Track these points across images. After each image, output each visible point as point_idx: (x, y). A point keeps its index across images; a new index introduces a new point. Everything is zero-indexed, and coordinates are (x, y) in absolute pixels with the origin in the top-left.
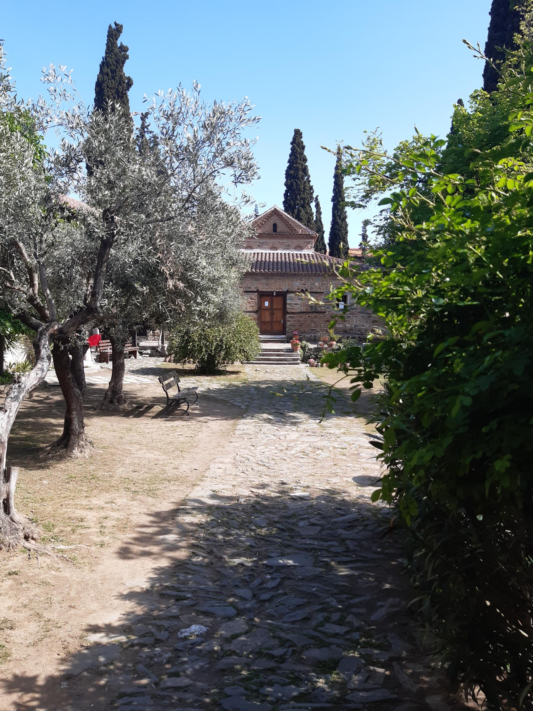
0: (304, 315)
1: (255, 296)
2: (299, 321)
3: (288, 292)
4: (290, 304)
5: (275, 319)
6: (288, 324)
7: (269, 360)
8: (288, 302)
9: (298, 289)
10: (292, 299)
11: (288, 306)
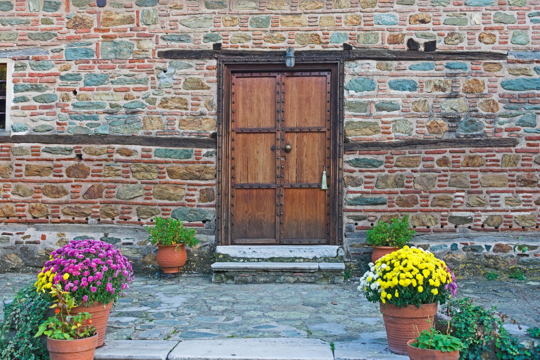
0: (422, 152)
1: (206, 72)
3: (349, 53)
5: (292, 176)
6: (350, 193)
9: (394, 40)
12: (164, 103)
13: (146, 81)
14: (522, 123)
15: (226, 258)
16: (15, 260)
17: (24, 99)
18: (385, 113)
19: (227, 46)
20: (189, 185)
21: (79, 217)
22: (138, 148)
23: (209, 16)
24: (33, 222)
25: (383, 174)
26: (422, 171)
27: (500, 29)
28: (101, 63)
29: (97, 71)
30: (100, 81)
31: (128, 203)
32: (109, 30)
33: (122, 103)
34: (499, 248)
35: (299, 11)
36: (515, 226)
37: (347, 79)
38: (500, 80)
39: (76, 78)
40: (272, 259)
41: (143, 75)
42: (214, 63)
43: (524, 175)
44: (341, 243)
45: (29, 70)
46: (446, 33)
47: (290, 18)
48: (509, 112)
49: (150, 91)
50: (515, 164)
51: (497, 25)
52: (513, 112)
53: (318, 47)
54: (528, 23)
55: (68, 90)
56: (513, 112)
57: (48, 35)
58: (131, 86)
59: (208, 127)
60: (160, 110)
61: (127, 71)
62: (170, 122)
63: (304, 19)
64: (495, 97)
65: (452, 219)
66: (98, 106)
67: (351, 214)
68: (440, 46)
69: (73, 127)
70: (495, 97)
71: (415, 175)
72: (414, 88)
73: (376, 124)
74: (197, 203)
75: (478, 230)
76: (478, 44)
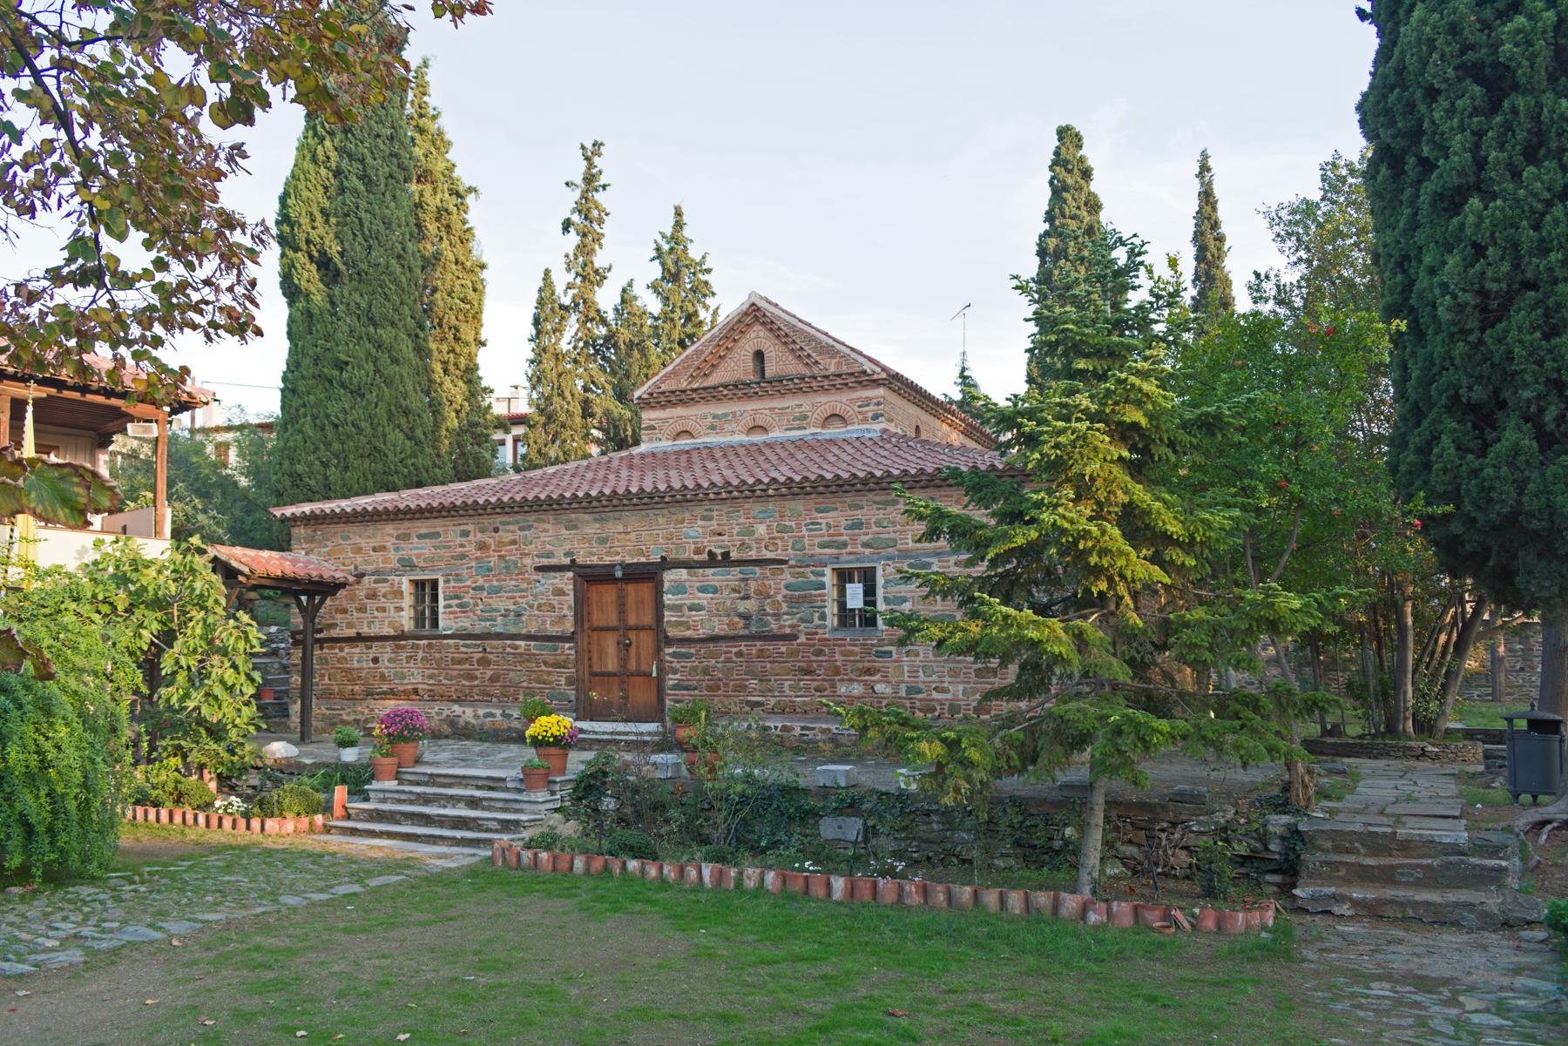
0: (723, 646)
1: (566, 581)
2: (706, 671)
3: (666, 564)
4: (676, 608)
5: (632, 665)
6: (671, 680)
7: (426, 820)
8: (668, 599)
9: (698, 551)
10: (680, 589)
11: (668, 616)
12: (539, 607)
13: (525, 590)
14: (802, 620)
16: (446, 729)
17: (449, 606)
19: (580, 561)
21: (486, 698)
22: (522, 643)
24: (457, 701)
27: (781, 538)
30: (498, 590)
31: (517, 686)
33: (512, 607)
34: (785, 728)
37: (666, 585)
39: (481, 588)
41: (524, 586)
42: (571, 574)
45: (452, 584)
53: (643, 560)
54: (804, 531)
57: (463, 556)
59: (569, 627)
62: (544, 622)
64: (780, 598)
65: (748, 703)
68: (734, 555)
69: (481, 627)
70: (780, 598)
72: (715, 591)
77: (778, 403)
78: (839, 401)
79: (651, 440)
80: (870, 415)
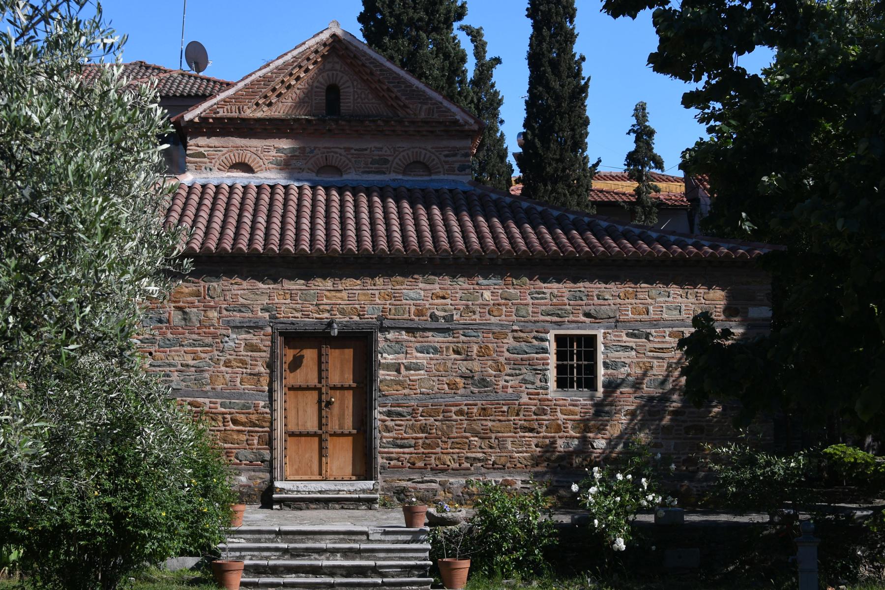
9: (420, 313)
15: (282, 490)
18: (412, 372)
20: (249, 432)
22: (207, 400)
23: (264, 291)
25: (411, 423)
26: (441, 421)
28: (174, 329)
29: (170, 336)
32: (179, 302)
33: (191, 363)
35: (340, 288)
36: (519, 465)
38: (506, 346)
40: (320, 492)
41: (209, 340)
43: (526, 424)
44: (376, 479)
46: (462, 308)
47: (333, 293)
48: (514, 372)
49: (216, 353)
50: (518, 415)
51: (503, 301)
52: (517, 372)
53: (356, 318)
55: (146, 352)
56: (517, 372)
58: (199, 349)
60: (223, 369)
61: (195, 337)
63: (344, 294)
66: (170, 365)
67: (385, 455)
71: (437, 423)
73: (405, 381)
74: (256, 446)
75: (488, 469)
76: (488, 316)
77: (355, 145)
78: (425, 149)
79: (198, 168)
80: (457, 165)
